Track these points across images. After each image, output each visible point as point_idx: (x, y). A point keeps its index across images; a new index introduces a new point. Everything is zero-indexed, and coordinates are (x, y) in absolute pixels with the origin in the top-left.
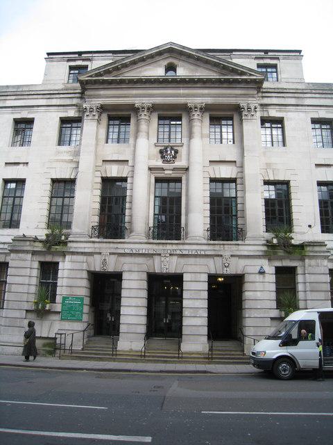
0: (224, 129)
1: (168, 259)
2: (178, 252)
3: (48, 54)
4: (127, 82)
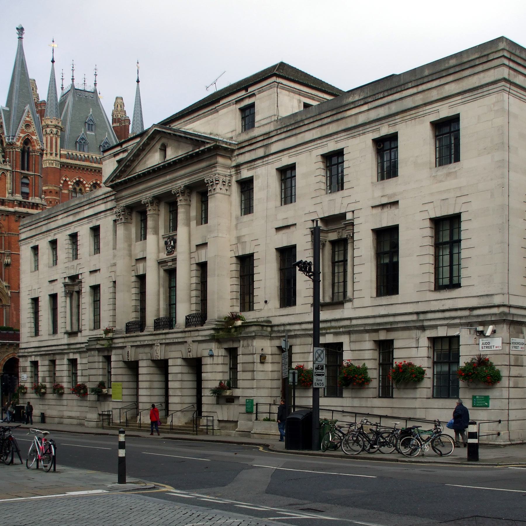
1: (159, 347)
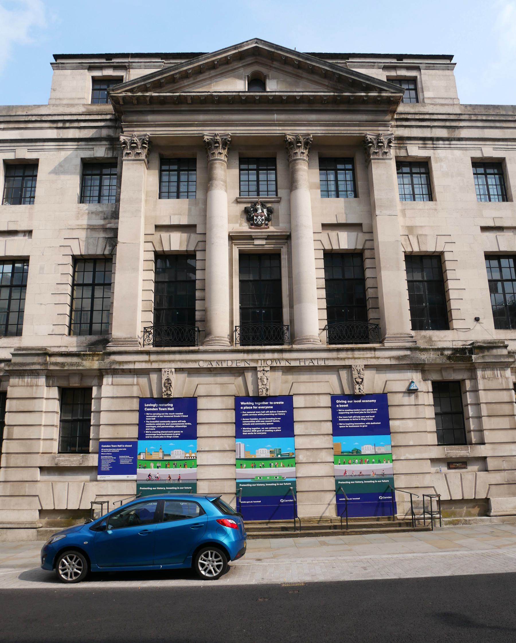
0: (341, 177)
1: (268, 374)
2: (283, 364)
3: (56, 57)
4: (190, 101)
